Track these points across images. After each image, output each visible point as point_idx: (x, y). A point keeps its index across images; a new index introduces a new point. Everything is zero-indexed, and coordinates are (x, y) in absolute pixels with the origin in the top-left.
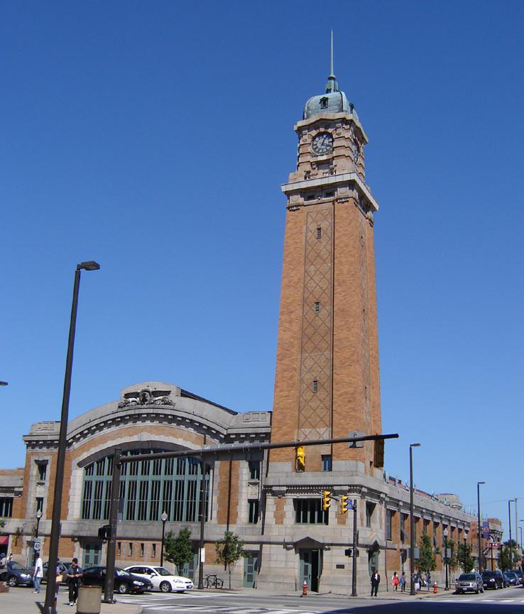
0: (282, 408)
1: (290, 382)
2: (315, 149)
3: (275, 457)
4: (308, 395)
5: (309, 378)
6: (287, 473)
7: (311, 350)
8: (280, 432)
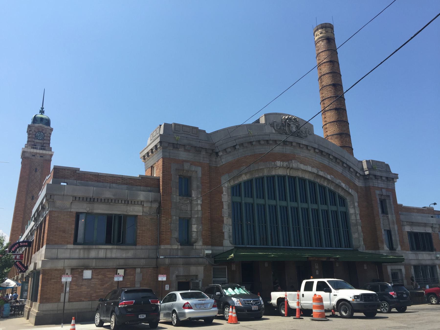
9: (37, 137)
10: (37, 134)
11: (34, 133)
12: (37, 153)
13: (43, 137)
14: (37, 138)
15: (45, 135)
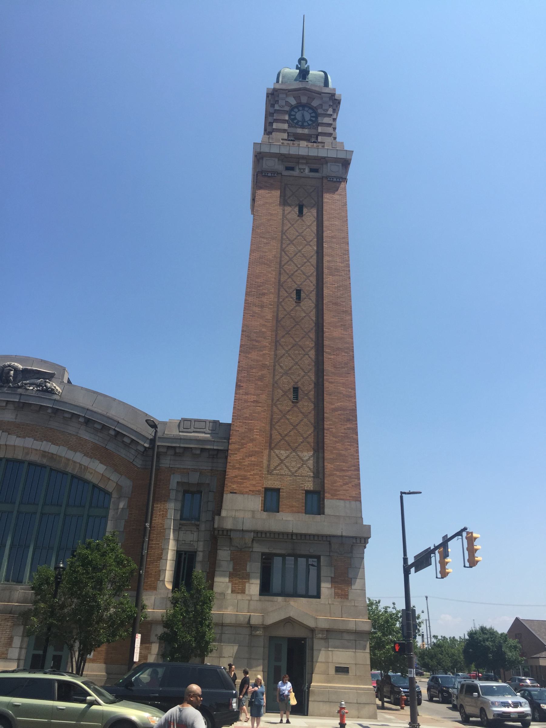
0: (246, 418)
1: (259, 383)
2: (293, 120)
3: (234, 486)
4: (286, 405)
5: (287, 383)
6: (253, 512)
7: (290, 347)
8: (244, 450)
9: (295, 121)
10: (293, 113)
11: (287, 108)
12: (298, 159)
13: (314, 119)
14: (293, 122)
15: (320, 111)
